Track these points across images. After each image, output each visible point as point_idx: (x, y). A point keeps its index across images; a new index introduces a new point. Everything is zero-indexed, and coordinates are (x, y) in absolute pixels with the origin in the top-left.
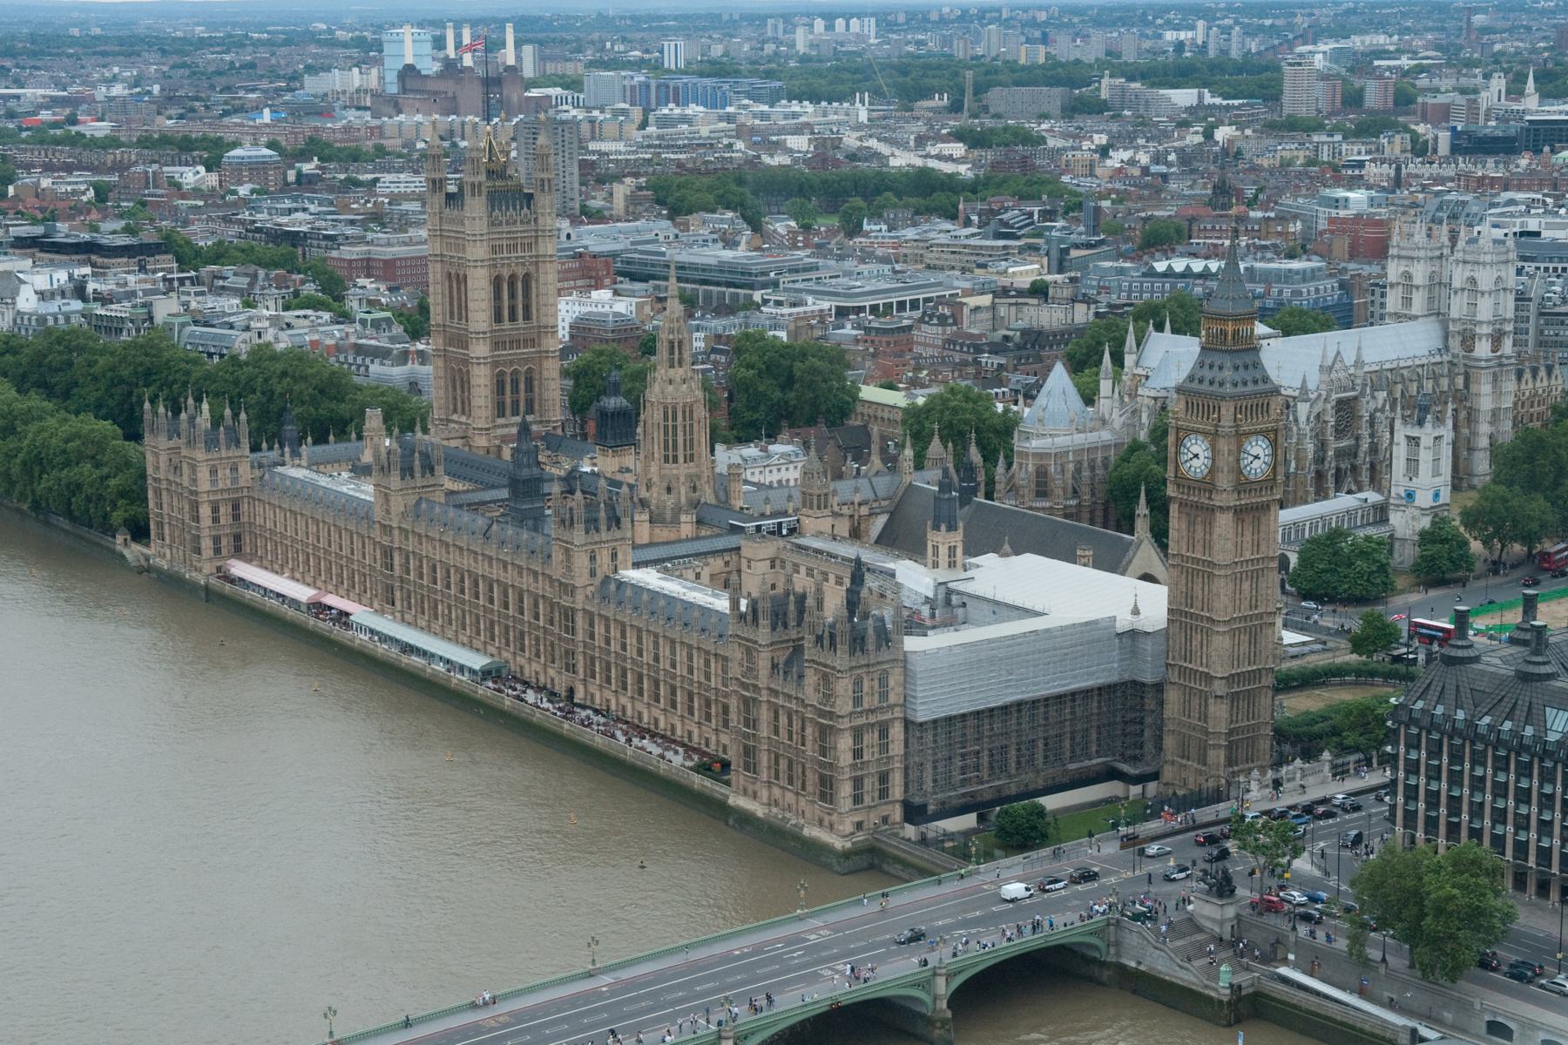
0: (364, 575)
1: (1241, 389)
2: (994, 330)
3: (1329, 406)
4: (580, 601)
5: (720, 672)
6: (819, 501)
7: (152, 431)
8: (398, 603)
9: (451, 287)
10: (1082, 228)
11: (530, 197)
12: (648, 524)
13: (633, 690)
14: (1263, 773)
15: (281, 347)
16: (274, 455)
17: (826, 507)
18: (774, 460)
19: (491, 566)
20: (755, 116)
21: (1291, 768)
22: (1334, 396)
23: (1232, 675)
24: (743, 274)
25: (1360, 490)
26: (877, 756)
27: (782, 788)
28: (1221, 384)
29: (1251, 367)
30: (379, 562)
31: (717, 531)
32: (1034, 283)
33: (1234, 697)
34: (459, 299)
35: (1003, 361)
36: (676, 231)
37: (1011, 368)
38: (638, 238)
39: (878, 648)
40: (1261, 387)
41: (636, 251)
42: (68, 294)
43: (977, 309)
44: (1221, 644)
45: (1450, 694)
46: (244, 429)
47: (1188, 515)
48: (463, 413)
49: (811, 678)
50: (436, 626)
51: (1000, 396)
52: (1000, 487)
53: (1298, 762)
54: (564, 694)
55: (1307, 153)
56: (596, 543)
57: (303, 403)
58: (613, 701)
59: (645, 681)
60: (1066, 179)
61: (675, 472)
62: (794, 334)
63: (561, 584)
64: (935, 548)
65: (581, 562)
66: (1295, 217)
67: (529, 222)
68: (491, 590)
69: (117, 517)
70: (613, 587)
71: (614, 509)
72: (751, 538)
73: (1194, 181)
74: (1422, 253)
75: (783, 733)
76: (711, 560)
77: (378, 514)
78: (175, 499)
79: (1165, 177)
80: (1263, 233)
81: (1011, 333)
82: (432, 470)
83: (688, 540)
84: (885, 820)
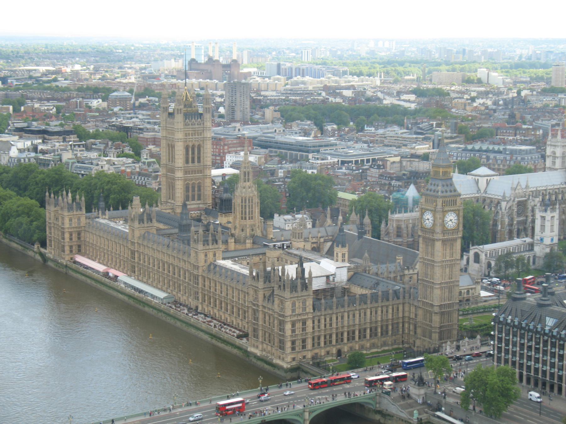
0: (125, 261)
1: (445, 194)
2: (401, 171)
3: (514, 203)
4: (200, 272)
6: (299, 235)
7: (49, 204)
8: (136, 272)
9: (169, 149)
10: (449, 131)
11: (201, 114)
12: (233, 244)
17: (301, 238)
19: (169, 258)
20: (333, 81)
22: (516, 200)
23: (441, 305)
24: (305, 146)
25: (527, 236)
26: (301, 332)
27: (267, 344)
28: (438, 192)
29: (449, 186)
31: (259, 246)
32: (424, 154)
33: (442, 314)
35: (400, 184)
36: (284, 129)
39: (302, 290)
40: (453, 193)
42: (31, 150)
43: (394, 162)
44: (437, 292)
45: (514, 311)
47: (426, 242)
48: (173, 199)
50: (150, 282)
52: (383, 233)
53: (467, 339)
54: (194, 308)
55: (556, 102)
57: (115, 193)
58: (212, 311)
59: (223, 303)
60: (453, 110)
62: (320, 171)
63: (194, 265)
64: (337, 254)
65: (202, 257)
66: (539, 128)
67: (200, 124)
68: (169, 268)
69: (36, 237)
70: (212, 267)
71: (215, 236)
72: (271, 249)
73: (505, 113)
74: (559, 144)
76: (254, 258)
77: (130, 237)
79: (495, 111)
81: (406, 173)
82: (151, 221)
83: (249, 249)
84: (304, 357)
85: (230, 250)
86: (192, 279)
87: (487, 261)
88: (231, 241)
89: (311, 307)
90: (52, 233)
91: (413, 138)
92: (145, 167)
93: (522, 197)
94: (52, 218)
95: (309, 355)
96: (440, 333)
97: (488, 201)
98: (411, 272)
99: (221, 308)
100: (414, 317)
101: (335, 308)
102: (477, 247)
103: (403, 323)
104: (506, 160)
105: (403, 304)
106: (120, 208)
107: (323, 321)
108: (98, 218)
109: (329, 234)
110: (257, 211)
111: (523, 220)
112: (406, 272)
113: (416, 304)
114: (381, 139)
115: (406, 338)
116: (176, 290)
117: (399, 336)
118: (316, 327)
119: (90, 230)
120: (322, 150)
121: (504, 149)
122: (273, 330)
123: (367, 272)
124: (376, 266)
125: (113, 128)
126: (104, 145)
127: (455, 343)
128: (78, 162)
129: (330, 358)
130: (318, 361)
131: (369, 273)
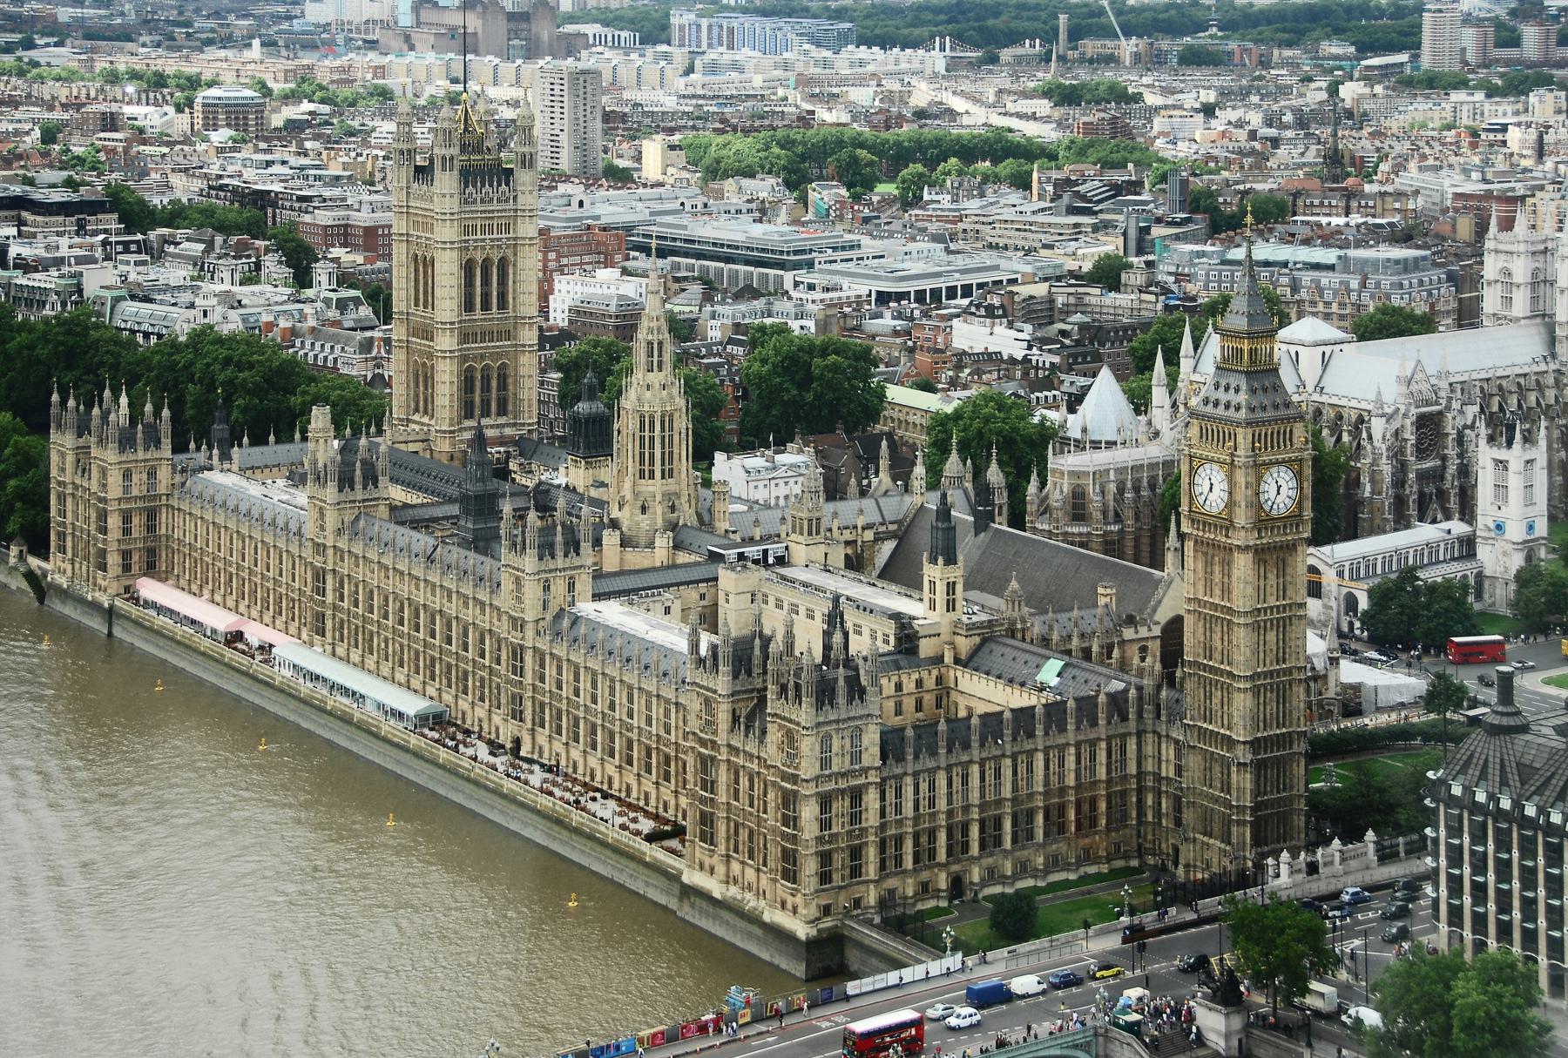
3: (1408, 422)
5: (681, 723)
7: (59, 426)
8: (329, 634)
13: (585, 744)
14: (1295, 856)
15: (225, 329)
16: (201, 457)
18: (781, 473)
21: (1329, 850)
22: (1414, 411)
25: (1448, 517)
27: (743, 863)
30: (310, 585)
34: (426, 284)
35: (1056, 359)
36: (705, 200)
38: (658, 207)
39: (850, 701)
46: (165, 427)
48: (426, 412)
49: (774, 735)
50: (370, 662)
51: (1042, 402)
53: (1336, 842)
54: (509, 746)
56: (551, 571)
61: (651, 489)
62: (823, 326)
63: (511, 617)
64: (932, 583)
65: (532, 591)
70: (566, 623)
77: (310, 530)
79: (1275, 143)
80: (1379, 209)
81: (1068, 327)
83: (662, 568)
86: (504, 657)
87: (1345, 591)
88: (610, 539)
89: (876, 750)
90: (69, 514)
92: (333, 314)
93: (1428, 403)
94: (69, 466)
95: (872, 897)
96: (1257, 826)
97: (1329, 414)
98: (1143, 632)
99: (594, 747)
100: (1171, 775)
101: (942, 751)
103: (1140, 791)
104: (1349, 291)
105: (1140, 734)
106: (272, 438)
107: (909, 791)
108: (211, 469)
109: (888, 518)
110: (683, 451)
111: (1434, 469)
112: (1129, 633)
113: (1177, 734)
115: (1150, 837)
116: (453, 691)
117: (1127, 831)
119: (185, 506)
121: (1340, 258)
122: (759, 821)
123: (1019, 635)
124: (1042, 618)
125: (222, 194)
126: (202, 247)
127: (1303, 854)
128: (133, 297)
129: (931, 904)
130: (900, 911)
131: (1024, 640)
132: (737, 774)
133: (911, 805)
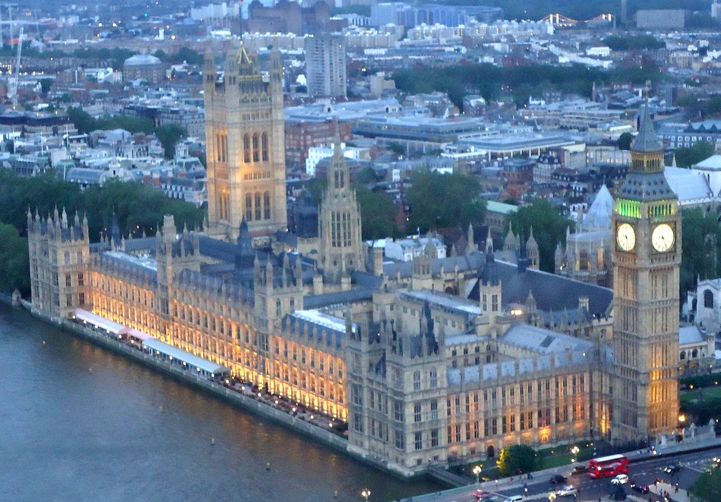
17: (428, 273)
27: (376, 440)
36: (401, 106)
37: (591, 190)
39: (430, 353)
41: (371, 119)
43: (575, 153)
49: (390, 371)
60: (671, 70)
63: (260, 320)
64: (485, 296)
67: (266, 100)
70: (288, 322)
75: (376, 406)
76: (354, 305)
78: (45, 271)
81: (594, 169)
82: (192, 253)
85: (316, 294)
86: (258, 341)
88: (318, 281)
90: (39, 276)
91: (606, 116)
92: (183, 170)
94: (38, 251)
95: (443, 456)
98: (603, 321)
102: (708, 281)
106: (144, 234)
108: (110, 250)
112: (595, 322)
113: (611, 371)
114: (555, 117)
118: (453, 411)
120: (461, 137)
125: (131, 111)
129: (476, 460)
130: (458, 464)
132: (372, 393)
133: (464, 408)
